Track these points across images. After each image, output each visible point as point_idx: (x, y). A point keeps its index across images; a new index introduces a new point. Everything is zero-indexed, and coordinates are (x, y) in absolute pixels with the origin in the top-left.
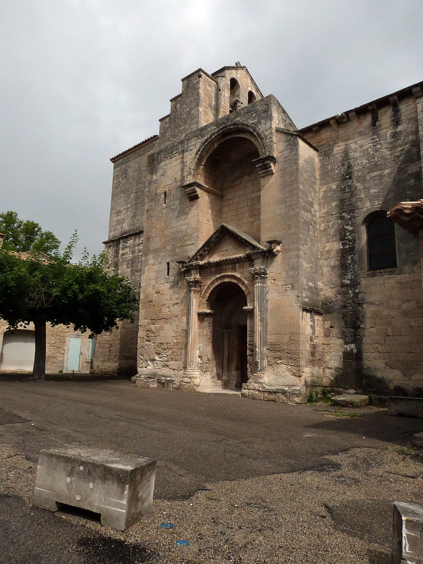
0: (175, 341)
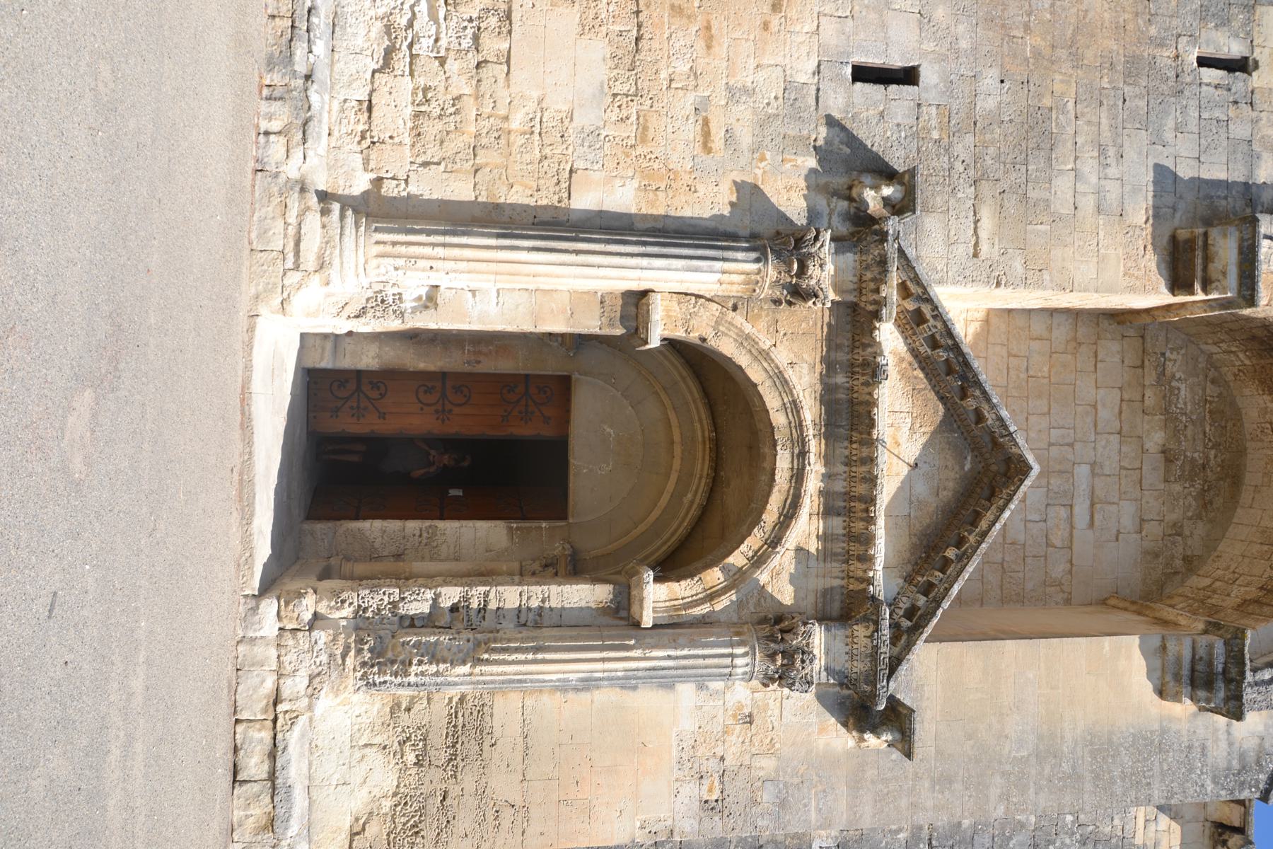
0: (516, 123)
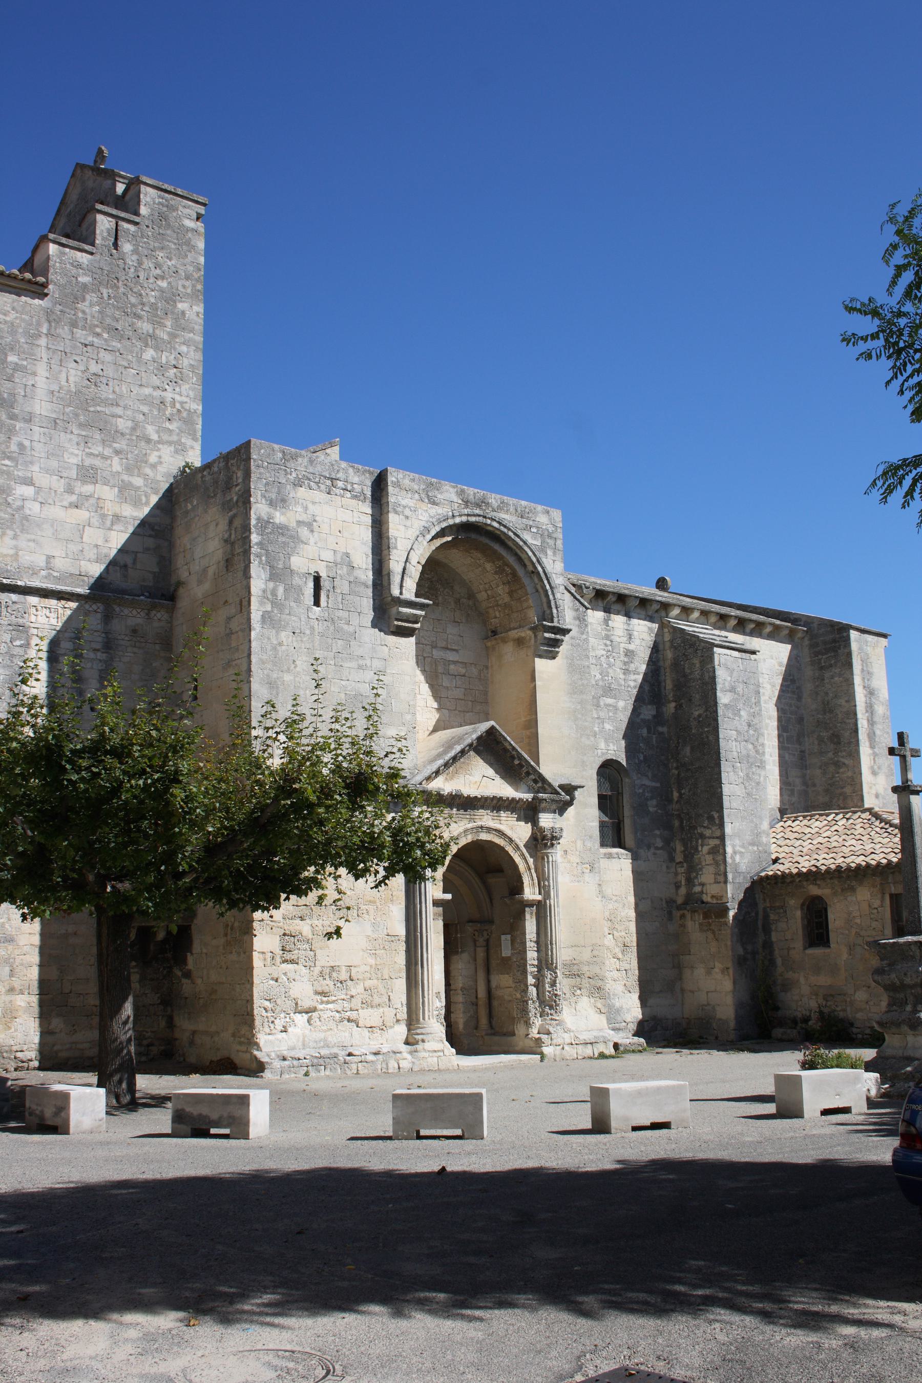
0: (372, 961)
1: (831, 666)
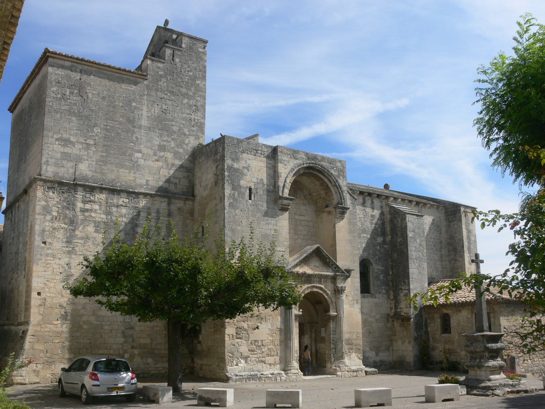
1: (453, 221)
